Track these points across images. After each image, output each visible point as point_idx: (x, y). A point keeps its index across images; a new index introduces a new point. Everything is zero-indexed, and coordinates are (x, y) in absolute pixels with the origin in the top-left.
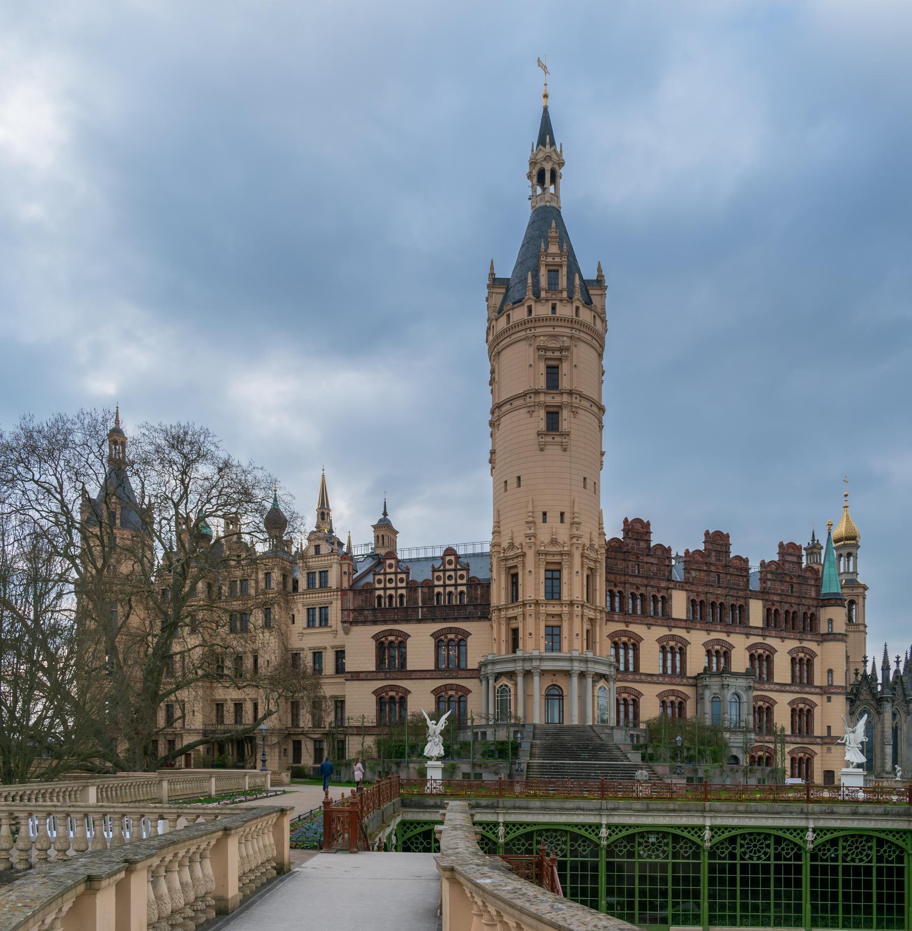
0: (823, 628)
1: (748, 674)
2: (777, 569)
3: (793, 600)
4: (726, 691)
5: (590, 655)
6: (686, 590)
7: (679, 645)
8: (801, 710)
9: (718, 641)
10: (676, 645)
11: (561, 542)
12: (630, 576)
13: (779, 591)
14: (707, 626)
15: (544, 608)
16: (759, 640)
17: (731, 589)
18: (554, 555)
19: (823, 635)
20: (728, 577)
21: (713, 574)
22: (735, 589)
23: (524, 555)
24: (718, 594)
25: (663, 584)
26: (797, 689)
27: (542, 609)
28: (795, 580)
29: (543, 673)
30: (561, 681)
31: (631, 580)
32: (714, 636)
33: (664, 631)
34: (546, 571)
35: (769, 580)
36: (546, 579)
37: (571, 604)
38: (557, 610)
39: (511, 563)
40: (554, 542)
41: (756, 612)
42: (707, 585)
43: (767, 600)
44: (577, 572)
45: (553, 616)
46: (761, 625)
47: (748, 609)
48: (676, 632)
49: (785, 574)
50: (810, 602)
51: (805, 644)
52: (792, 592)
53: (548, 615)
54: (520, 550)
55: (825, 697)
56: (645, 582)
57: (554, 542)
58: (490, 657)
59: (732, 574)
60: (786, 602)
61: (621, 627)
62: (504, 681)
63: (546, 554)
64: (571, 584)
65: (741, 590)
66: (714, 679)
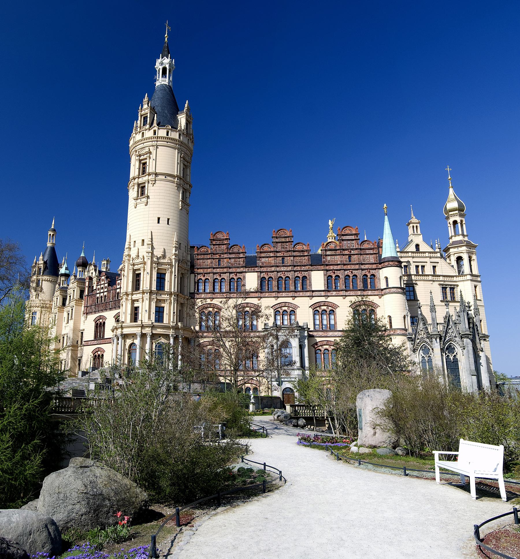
0: (383, 285)
3: (353, 267)
6: (256, 272)
12: (214, 268)
13: (339, 263)
14: (274, 294)
16: (323, 299)
17: (295, 266)
18: (138, 265)
19: (382, 290)
20: (292, 258)
24: (282, 271)
28: (353, 252)
35: (329, 255)
42: (273, 266)
43: (327, 271)
47: (310, 278)
48: (248, 300)
49: (344, 250)
50: (370, 266)
52: (350, 261)
59: (294, 256)
65: (303, 266)
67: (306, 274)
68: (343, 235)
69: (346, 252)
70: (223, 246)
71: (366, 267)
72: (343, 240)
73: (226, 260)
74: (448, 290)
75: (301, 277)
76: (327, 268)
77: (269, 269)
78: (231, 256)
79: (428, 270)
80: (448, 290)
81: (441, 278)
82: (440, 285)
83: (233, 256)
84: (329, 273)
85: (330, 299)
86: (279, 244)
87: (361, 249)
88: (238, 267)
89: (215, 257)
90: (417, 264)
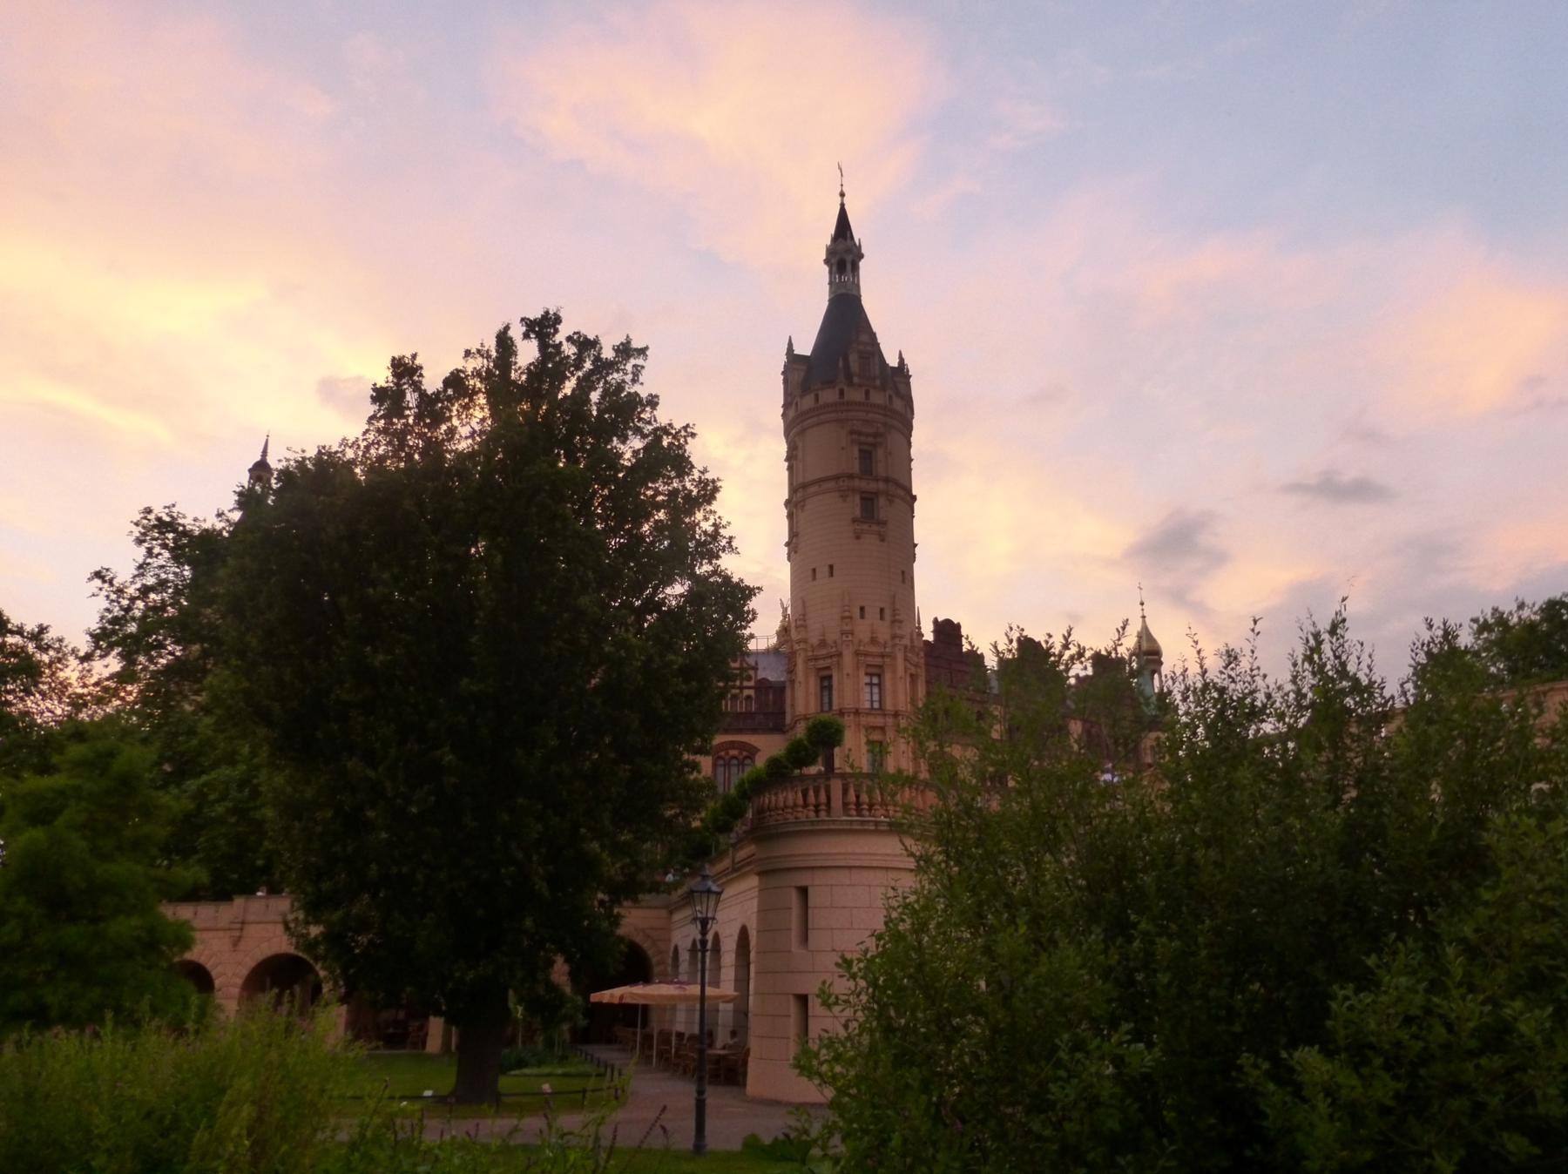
11: (882, 641)
15: (864, 719)
23: (840, 655)
27: (864, 720)
39: (821, 664)
40: (874, 641)
44: (901, 678)
45: (874, 728)
54: (834, 649)
57: (874, 641)
63: (866, 655)
64: (895, 692)
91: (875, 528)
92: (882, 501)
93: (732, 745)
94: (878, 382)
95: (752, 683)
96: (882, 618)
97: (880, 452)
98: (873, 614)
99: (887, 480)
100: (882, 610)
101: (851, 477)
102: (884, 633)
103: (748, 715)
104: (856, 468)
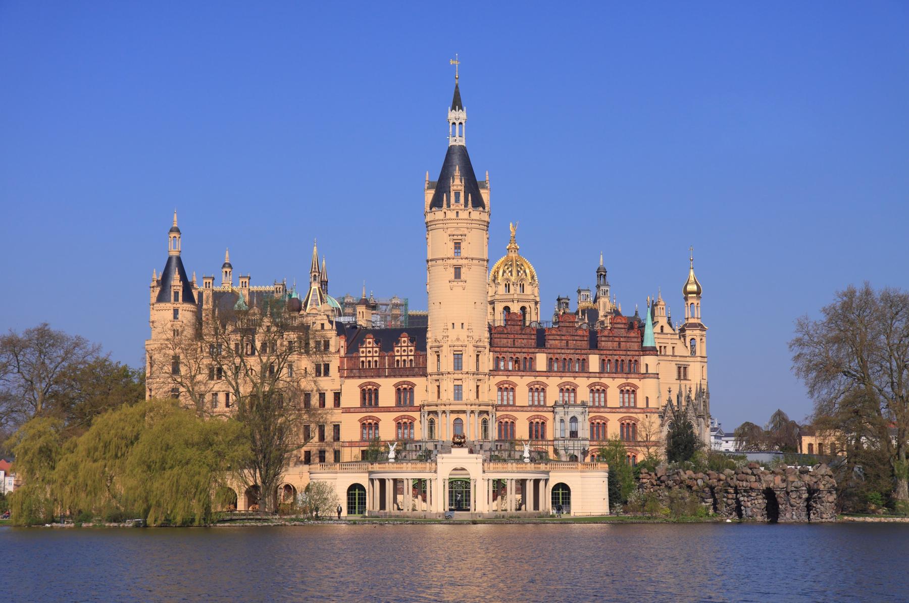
0: (643, 370)
1: (583, 404)
2: (609, 333)
3: (621, 353)
4: (566, 416)
5: (477, 402)
7: (542, 387)
8: (628, 424)
9: (568, 383)
10: (540, 387)
12: (510, 347)
13: (611, 348)
16: (597, 380)
17: (576, 349)
20: (574, 342)
21: (563, 341)
22: (579, 349)
25: (531, 350)
26: (624, 410)
28: (622, 339)
29: (452, 412)
30: (462, 416)
31: (510, 350)
32: (565, 379)
33: (532, 379)
34: (454, 354)
35: (603, 341)
36: (454, 359)
37: (467, 373)
38: (460, 376)
40: (458, 339)
41: (594, 362)
46: (598, 371)
48: (539, 379)
49: (615, 337)
50: (634, 353)
51: (630, 381)
52: (619, 347)
53: (455, 379)
55: (645, 415)
56: (519, 350)
57: (458, 339)
58: (426, 403)
59: (576, 340)
60: (615, 355)
61: (505, 378)
62: (431, 416)
66: (560, 408)
67: (584, 357)
68: (616, 323)
69: (617, 339)
70: (516, 327)
71: (632, 353)
72: (615, 328)
73: (519, 341)
74: (682, 369)
75: (581, 359)
76: (602, 352)
77: (555, 351)
78: (523, 337)
79: (669, 351)
80: (682, 369)
81: (678, 359)
82: (676, 364)
83: (525, 337)
84: (603, 357)
85: (603, 380)
86: (565, 329)
87: (628, 337)
88: (530, 348)
89: (510, 336)
90: (661, 345)
91: (460, 284)
92: (463, 270)
93: (404, 383)
94: (463, 207)
95: (412, 353)
96: (462, 327)
97: (463, 245)
98: (458, 326)
99: (467, 258)
100: (462, 324)
101: (449, 258)
102: (463, 334)
103: (411, 368)
104: (451, 252)
